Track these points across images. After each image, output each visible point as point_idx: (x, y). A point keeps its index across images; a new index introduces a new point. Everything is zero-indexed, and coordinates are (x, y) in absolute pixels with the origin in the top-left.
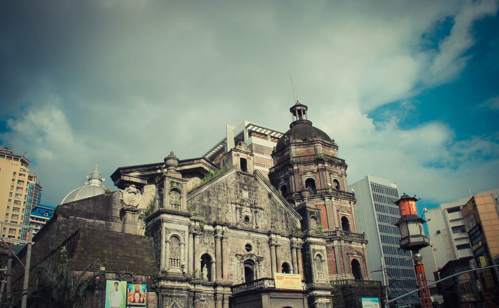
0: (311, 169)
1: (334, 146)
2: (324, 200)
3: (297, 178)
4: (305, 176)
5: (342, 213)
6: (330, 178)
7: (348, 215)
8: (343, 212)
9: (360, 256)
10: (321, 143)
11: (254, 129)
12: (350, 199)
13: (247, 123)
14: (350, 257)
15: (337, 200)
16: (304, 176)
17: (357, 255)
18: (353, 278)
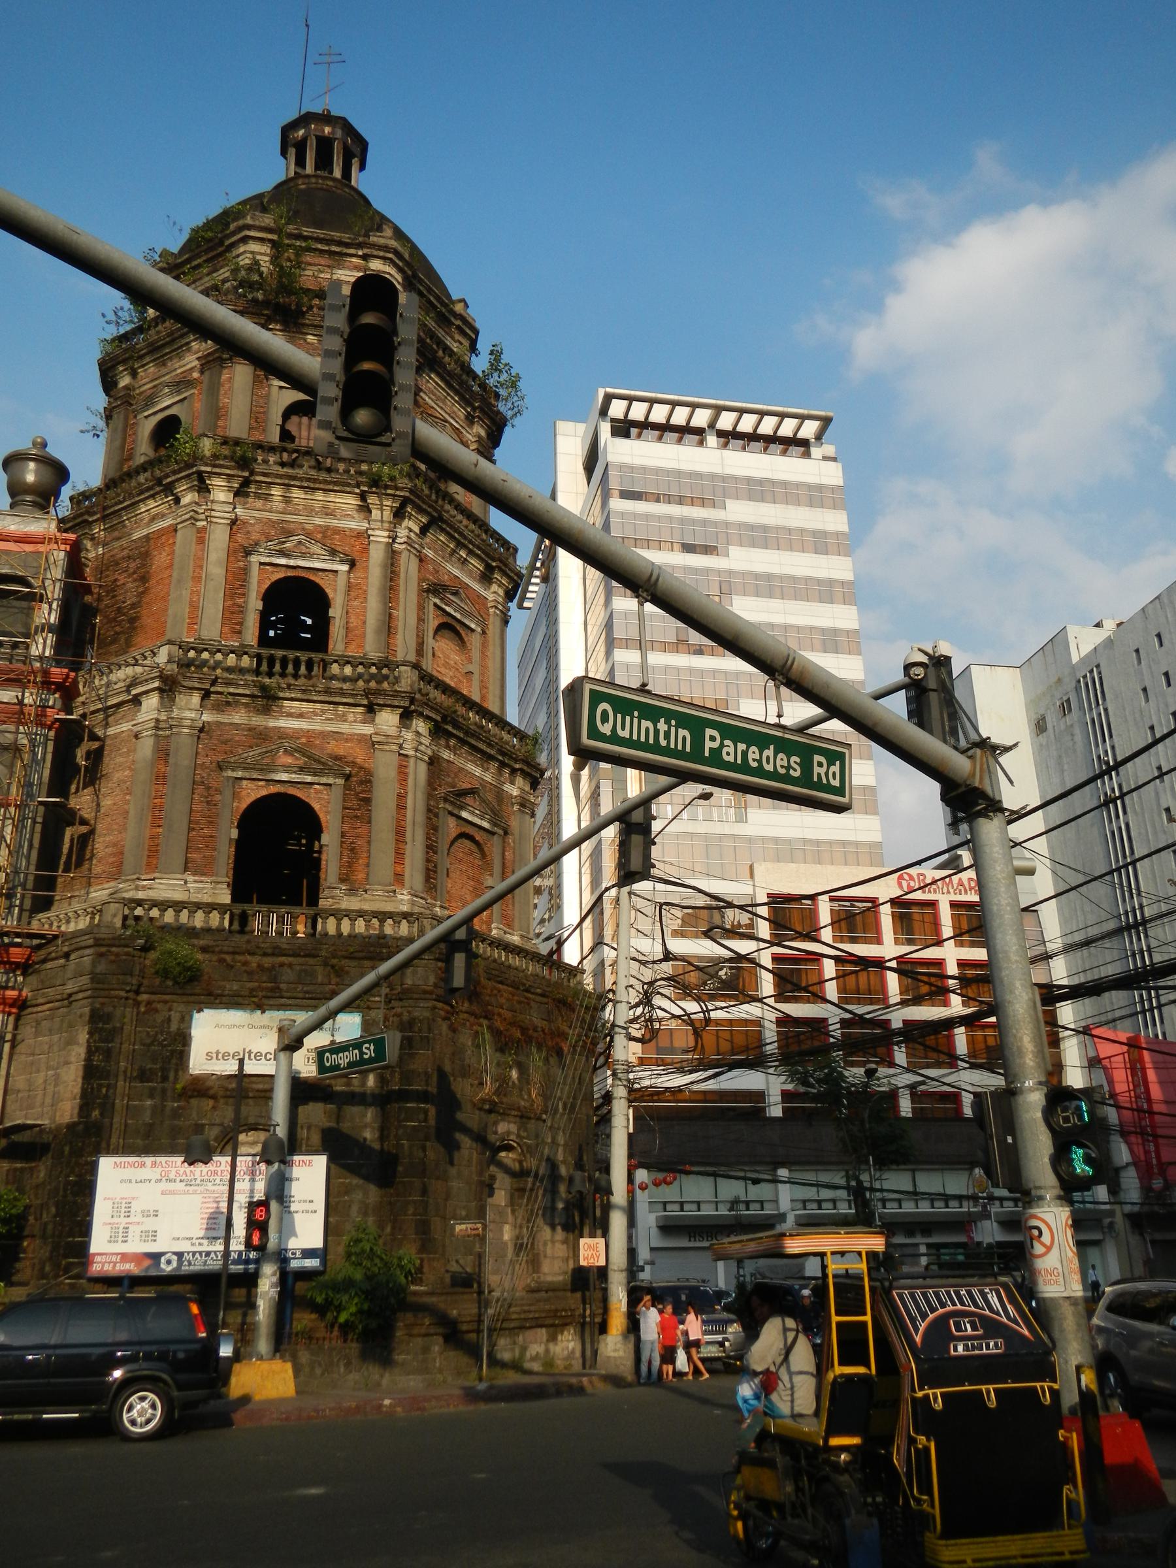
0: (179, 371)
1: (360, 246)
2: (177, 500)
3: (121, 426)
4: (150, 412)
5: (283, 561)
6: (267, 397)
7: (336, 572)
8: (283, 554)
9: (324, 780)
10: (261, 240)
11: (638, 412)
12: (358, 485)
13: (601, 393)
14: (245, 783)
15: (258, 496)
16: (146, 414)
17: (301, 770)
18: (225, 898)
